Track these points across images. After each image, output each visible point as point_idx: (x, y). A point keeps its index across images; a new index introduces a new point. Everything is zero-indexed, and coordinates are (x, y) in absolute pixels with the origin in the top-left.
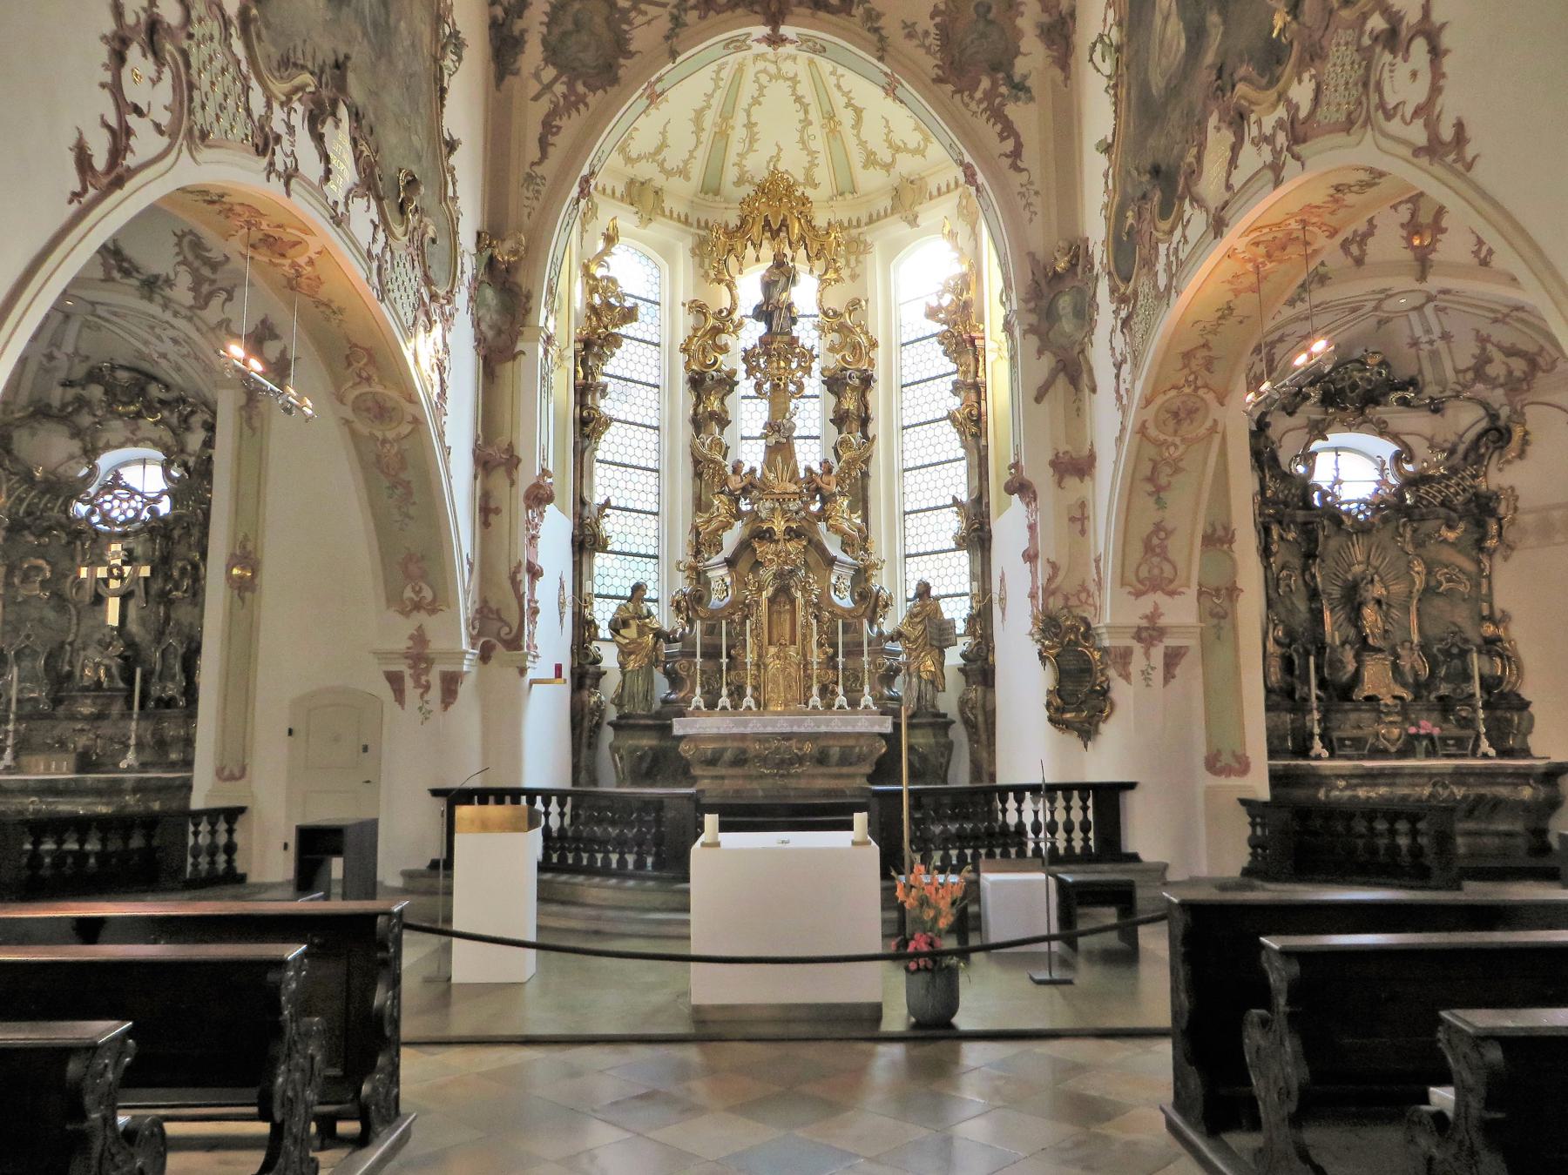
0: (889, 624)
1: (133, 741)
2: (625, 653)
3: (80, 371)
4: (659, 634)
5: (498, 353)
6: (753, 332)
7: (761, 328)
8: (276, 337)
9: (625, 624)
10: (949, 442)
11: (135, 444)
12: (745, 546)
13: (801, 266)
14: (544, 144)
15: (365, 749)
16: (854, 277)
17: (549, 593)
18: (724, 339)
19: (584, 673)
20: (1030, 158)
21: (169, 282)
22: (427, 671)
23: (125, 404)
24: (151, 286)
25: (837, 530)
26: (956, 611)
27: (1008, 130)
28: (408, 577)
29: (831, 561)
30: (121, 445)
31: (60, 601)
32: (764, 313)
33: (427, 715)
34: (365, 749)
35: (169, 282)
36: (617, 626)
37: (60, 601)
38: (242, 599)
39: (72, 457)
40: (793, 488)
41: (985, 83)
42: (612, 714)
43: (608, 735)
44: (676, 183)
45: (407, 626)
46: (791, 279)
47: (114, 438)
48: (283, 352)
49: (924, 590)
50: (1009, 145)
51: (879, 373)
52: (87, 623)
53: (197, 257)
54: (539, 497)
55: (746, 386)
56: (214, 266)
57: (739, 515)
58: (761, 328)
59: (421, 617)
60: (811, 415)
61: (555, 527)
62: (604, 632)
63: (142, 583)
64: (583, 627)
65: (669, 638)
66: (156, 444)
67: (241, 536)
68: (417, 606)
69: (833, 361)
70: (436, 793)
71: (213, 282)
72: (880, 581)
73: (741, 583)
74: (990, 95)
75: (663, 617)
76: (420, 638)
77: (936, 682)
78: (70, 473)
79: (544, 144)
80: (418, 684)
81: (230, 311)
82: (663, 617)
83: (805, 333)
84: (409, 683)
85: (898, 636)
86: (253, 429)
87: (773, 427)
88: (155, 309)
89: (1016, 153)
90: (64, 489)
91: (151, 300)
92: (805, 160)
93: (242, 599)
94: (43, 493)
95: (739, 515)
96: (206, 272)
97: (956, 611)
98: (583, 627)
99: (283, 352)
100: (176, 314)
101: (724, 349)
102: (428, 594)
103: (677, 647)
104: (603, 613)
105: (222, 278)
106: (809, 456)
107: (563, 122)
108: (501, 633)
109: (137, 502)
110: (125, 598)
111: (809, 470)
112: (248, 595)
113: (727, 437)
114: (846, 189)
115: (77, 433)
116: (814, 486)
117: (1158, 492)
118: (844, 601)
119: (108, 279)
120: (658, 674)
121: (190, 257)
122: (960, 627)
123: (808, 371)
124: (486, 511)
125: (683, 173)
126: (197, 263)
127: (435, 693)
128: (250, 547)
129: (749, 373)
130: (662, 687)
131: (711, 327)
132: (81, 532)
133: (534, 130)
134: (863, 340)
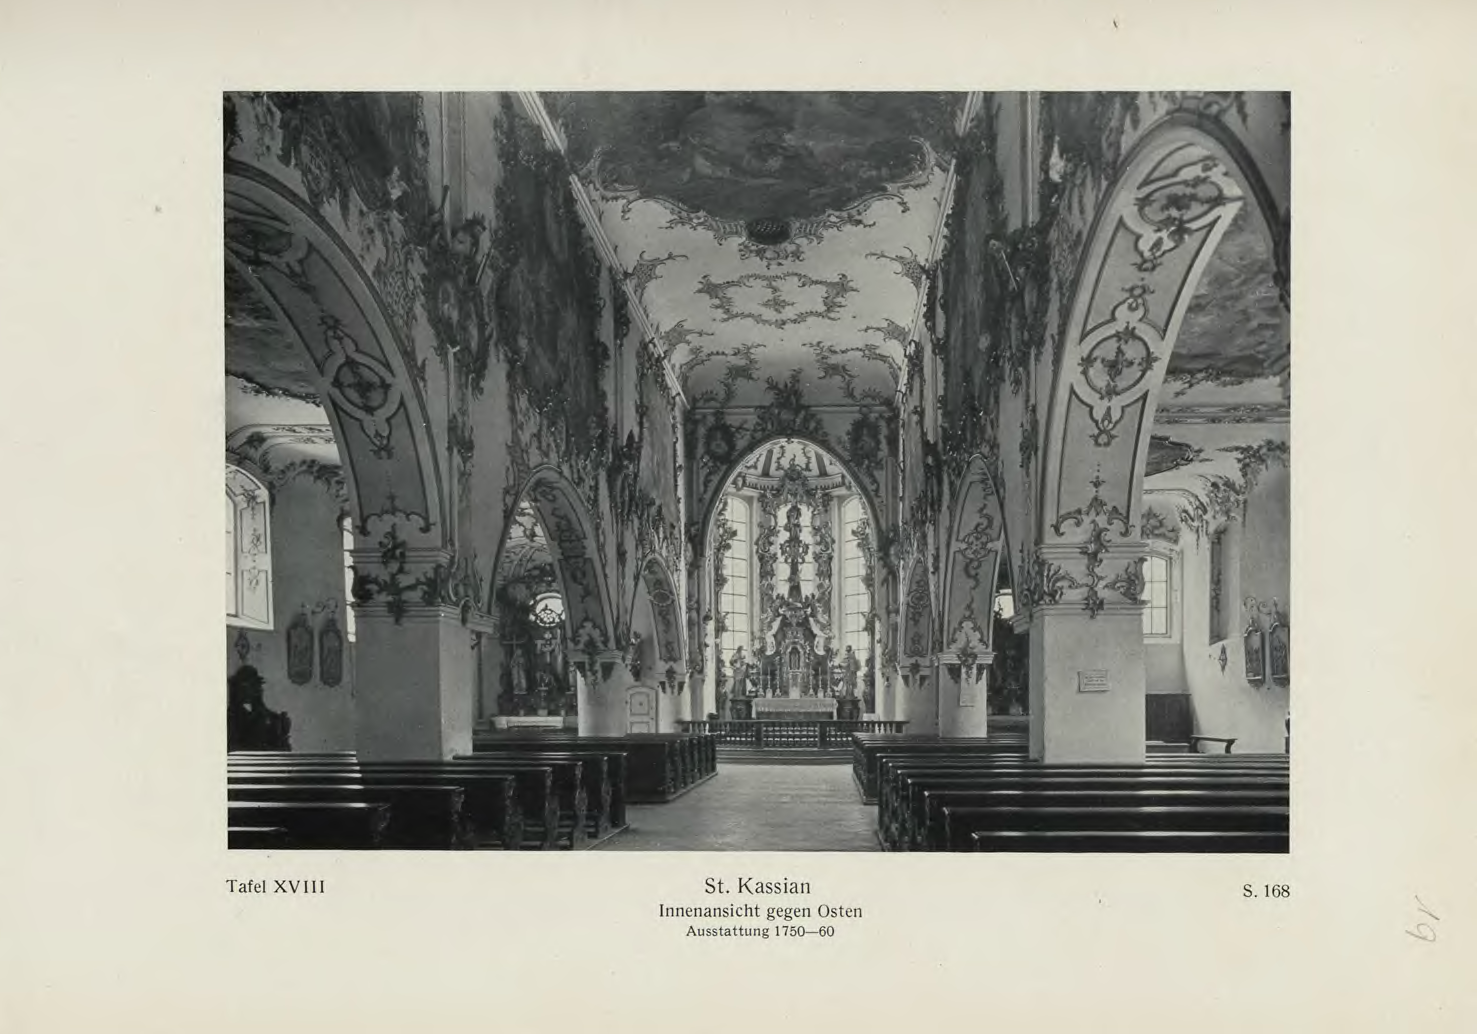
0: (837, 661)
2: (735, 671)
4: (748, 665)
5: (694, 567)
6: (784, 536)
7: (788, 534)
9: (736, 661)
10: (862, 588)
12: (781, 629)
13: (803, 508)
14: (706, 486)
16: (826, 511)
17: (709, 653)
18: (772, 539)
19: (720, 681)
20: (882, 492)
25: (817, 622)
26: (862, 657)
27: (875, 481)
29: (814, 636)
32: (787, 528)
36: (732, 663)
40: (799, 605)
41: (866, 462)
42: (730, 696)
43: (729, 704)
44: (752, 471)
46: (799, 513)
49: (849, 649)
50: (874, 487)
51: (835, 555)
54: (707, 618)
55: (781, 559)
57: (779, 615)
58: (788, 534)
60: (808, 570)
61: (711, 626)
62: (727, 664)
64: (720, 662)
65: (752, 667)
69: (818, 549)
72: (834, 645)
73: (779, 644)
74: (868, 467)
75: (749, 659)
77: (854, 685)
79: (706, 486)
82: (749, 659)
83: (806, 536)
85: (840, 667)
87: (790, 580)
89: (877, 491)
92: (805, 460)
95: (779, 615)
97: (862, 657)
98: (720, 662)
101: (771, 544)
103: (755, 671)
104: (727, 657)
106: (808, 589)
107: (712, 477)
108: (697, 667)
109: (554, 615)
111: (807, 597)
113: (774, 581)
114: (823, 473)
115: (529, 587)
116: (808, 603)
117: (916, 622)
118: (821, 652)
120: (748, 682)
122: (863, 663)
123: (806, 553)
124: (690, 623)
125: (755, 467)
129: (783, 554)
130: (749, 686)
131: (768, 533)
133: (702, 479)
134: (829, 540)
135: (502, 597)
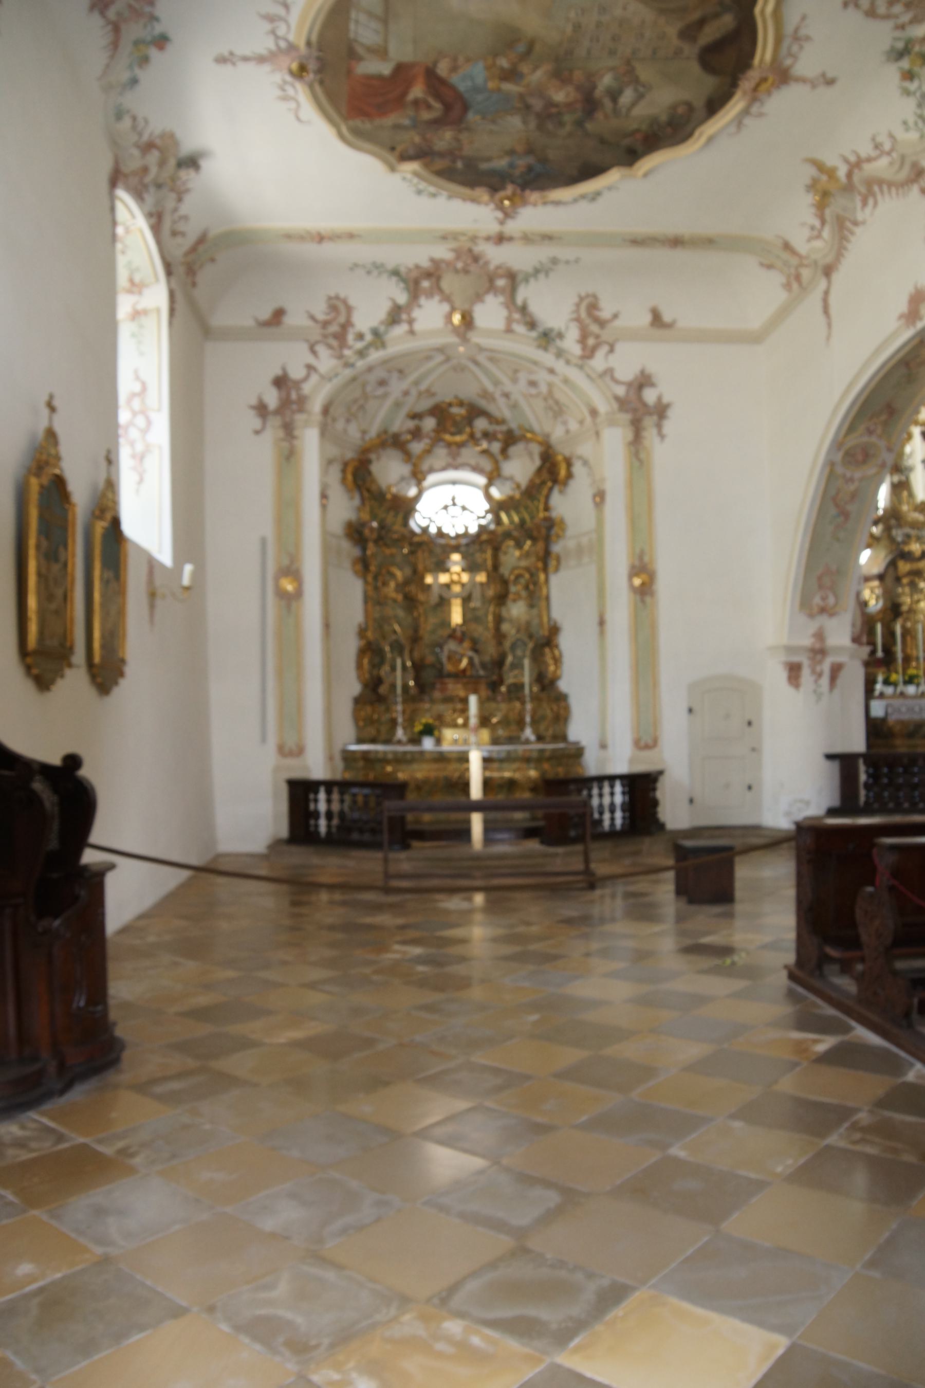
1: (528, 719)
3: (426, 404)
8: (652, 385)
11: (456, 468)
15: (750, 723)
21: (560, 336)
22: (820, 662)
23: (453, 434)
24: (547, 338)
28: (821, 587)
30: (444, 469)
31: (410, 602)
33: (819, 696)
34: (750, 723)
35: (560, 336)
37: (410, 602)
38: (643, 601)
39: (403, 479)
45: (813, 626)
47: (438, 463)
48: (660, 398)
52: (433, 620)
53: (590, 314)
56: (602, 324)
59: (823, 620)
63: (478, 589)
66: (476, 469)
67: (638, 551)
68: (823, 610)
70: (830, 757)
71: (597, 337)
76: (820, 635)
78: (402, 493)
80: (813, 672)
81: (614, 361)
84: (806, 673)
86: (640, 461)
88: (547, 358)
90: (406, 507)
91: (545, 349)
93: (643, 601)
94: (389, 509)
96: (594, 328)
99: (660, 398)
100: (568, 362)
102: (831, 600)
105: (606, 335)
110: (466, 600)
112: (648, 599)
119: (509, 330)
121: (583, 314)
126: (588, 321)
127: (825, 681)
128: (646, 559)
132: (420, 545)
135: (358, 474)
